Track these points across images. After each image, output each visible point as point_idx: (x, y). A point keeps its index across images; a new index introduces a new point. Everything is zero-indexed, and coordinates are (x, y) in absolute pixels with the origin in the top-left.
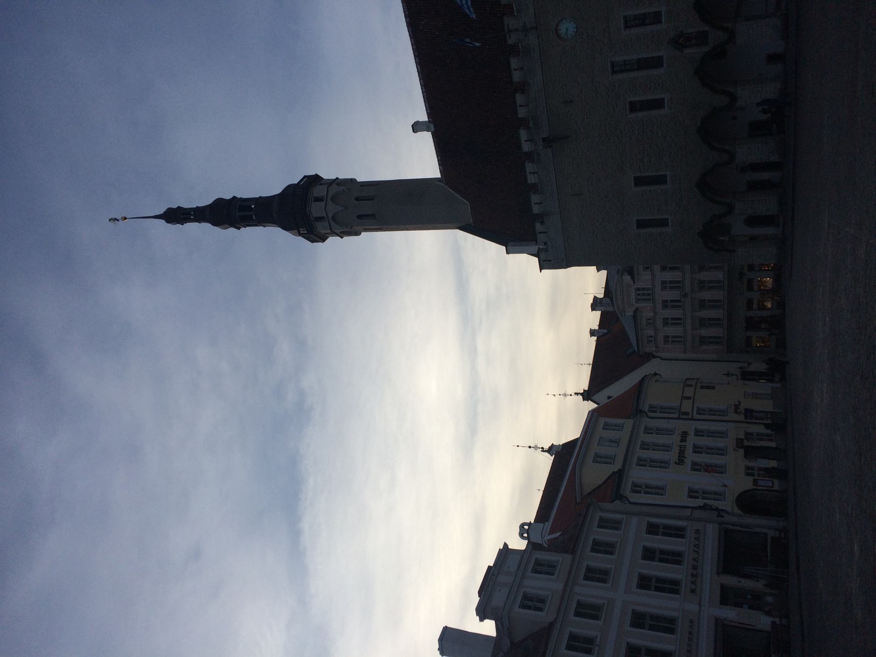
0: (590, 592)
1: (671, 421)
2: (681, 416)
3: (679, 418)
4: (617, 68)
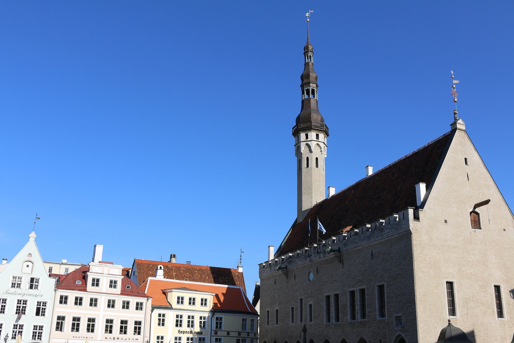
0: (103, 302)
1: (210, 327)
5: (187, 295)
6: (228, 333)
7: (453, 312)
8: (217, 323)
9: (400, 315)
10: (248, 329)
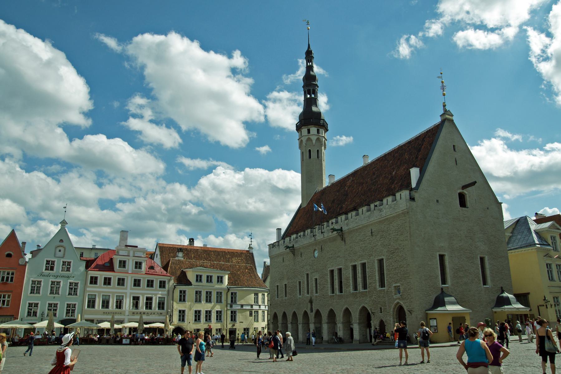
0: (129, 282)
4: (308, 275)
7: (444, 281)
8: (232, 298)
9: (398, 284)
10: (260, 303)
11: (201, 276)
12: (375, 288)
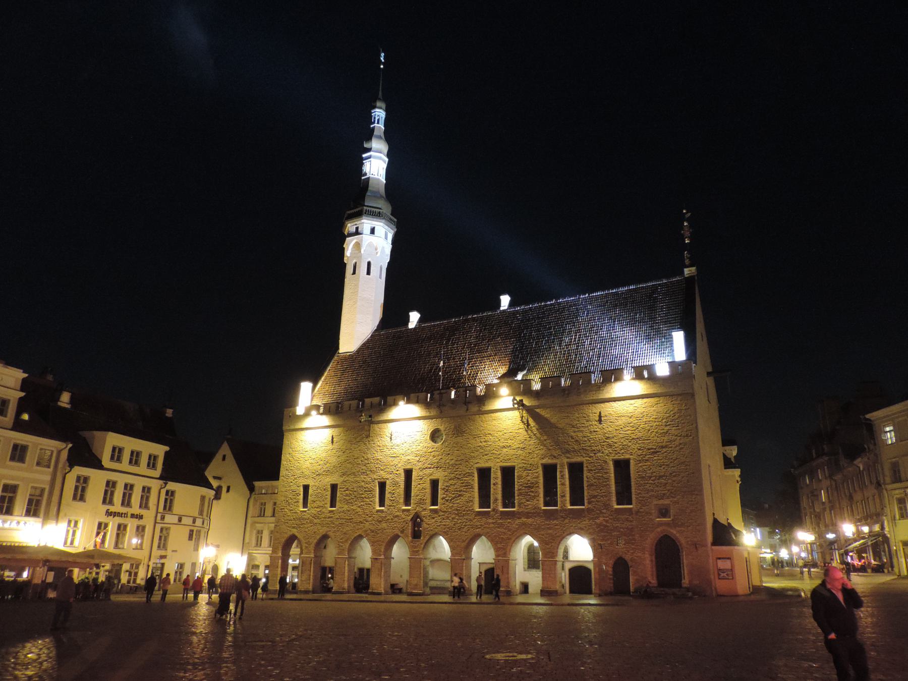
2: (159, 516)
3: (157, 512)
5: (129, 444)
6: (180, 520)
8: (166, 500)
11: (121, 450)
12: (607, 506)
